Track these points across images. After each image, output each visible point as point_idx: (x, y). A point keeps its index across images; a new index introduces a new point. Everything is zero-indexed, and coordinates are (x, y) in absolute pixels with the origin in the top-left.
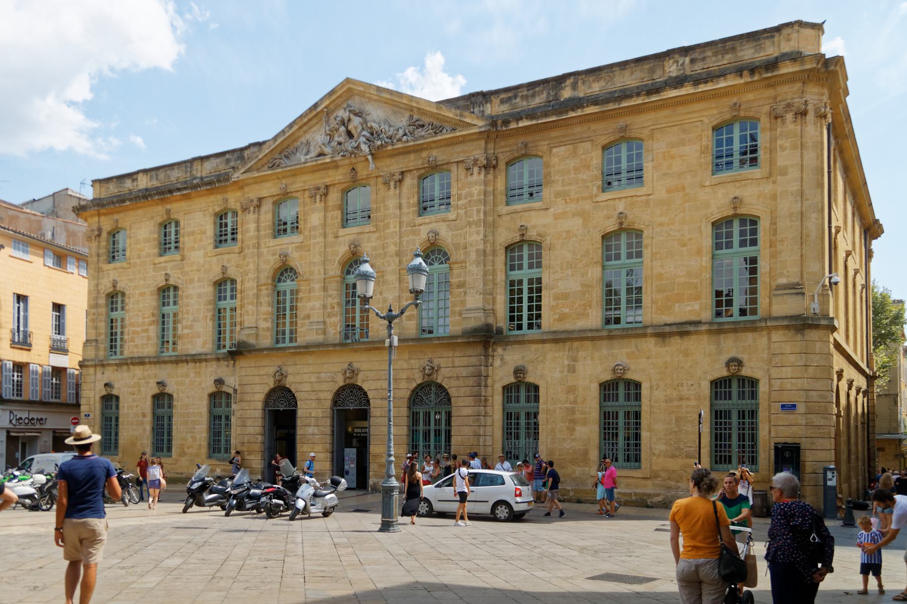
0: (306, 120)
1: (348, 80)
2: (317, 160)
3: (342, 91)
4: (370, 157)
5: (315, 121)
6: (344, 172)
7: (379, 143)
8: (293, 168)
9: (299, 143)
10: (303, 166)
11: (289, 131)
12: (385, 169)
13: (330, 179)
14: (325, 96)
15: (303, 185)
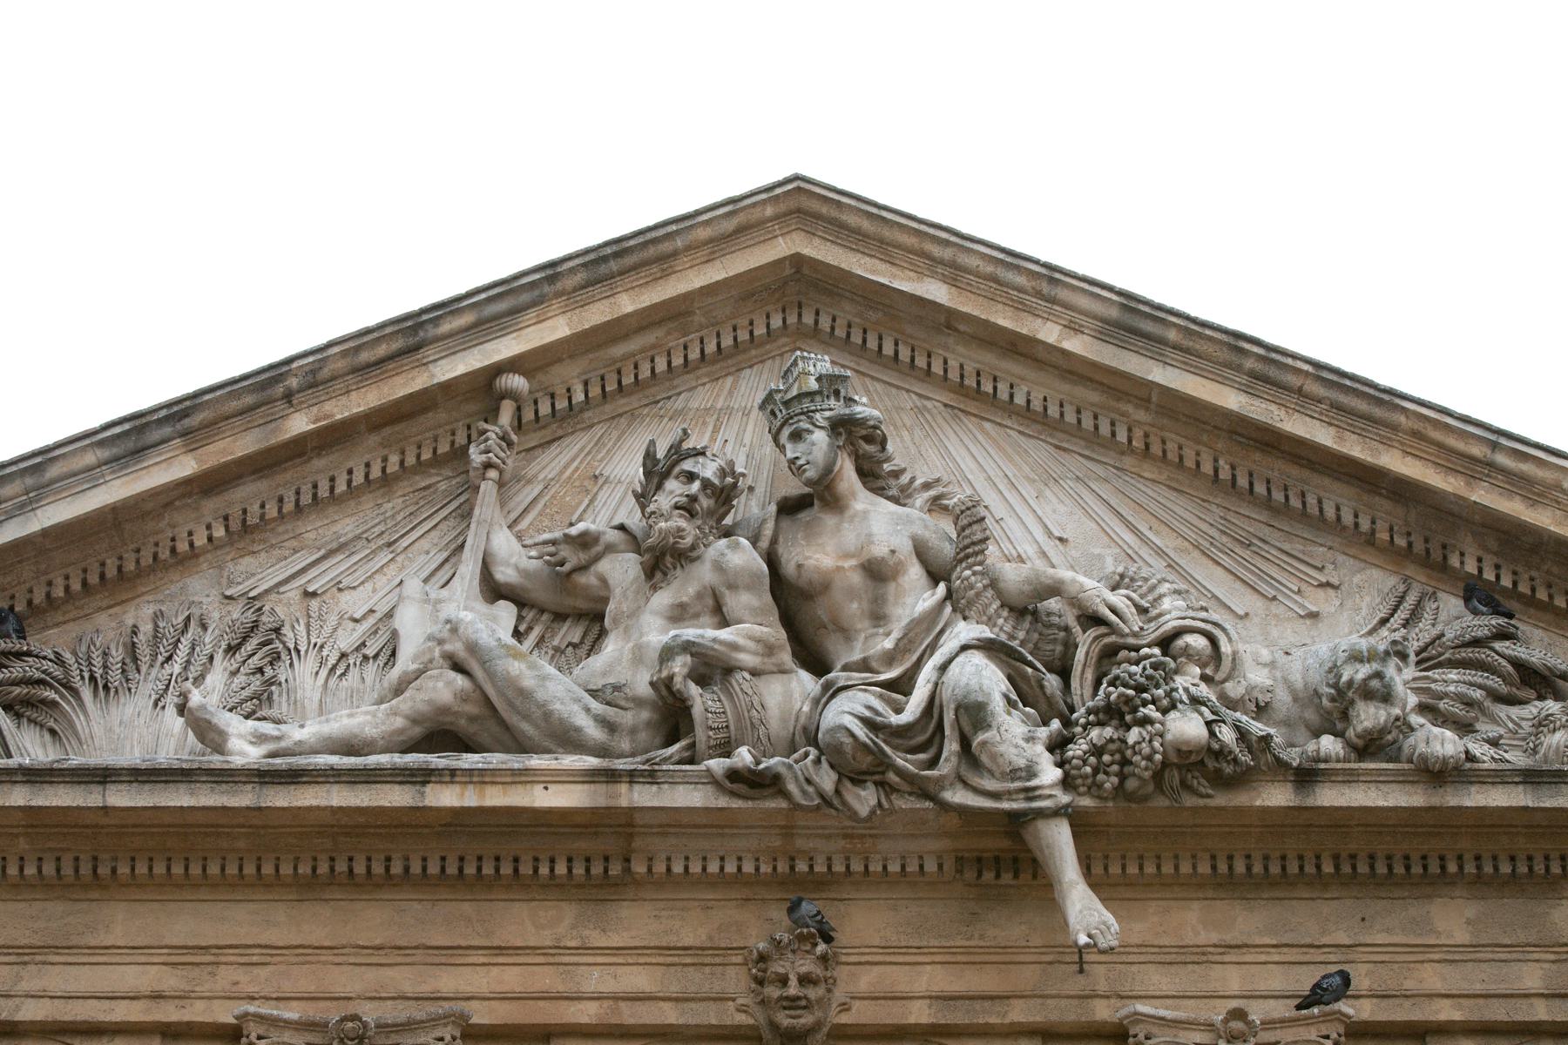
0: (299, 424)
1: (797, 178)
2: (424, 776)
3: (716, 273)
4: (1060, 840)
5: (359, 461)
6: (691, 932)
7: (1187, 727)
8: (120, 797)
9: (141, 614)
10: (243, 798)
11: (90, 476)
12: (1158, 979)
13: (510, 978)
14: (551, 271)
15: (170, 981)
